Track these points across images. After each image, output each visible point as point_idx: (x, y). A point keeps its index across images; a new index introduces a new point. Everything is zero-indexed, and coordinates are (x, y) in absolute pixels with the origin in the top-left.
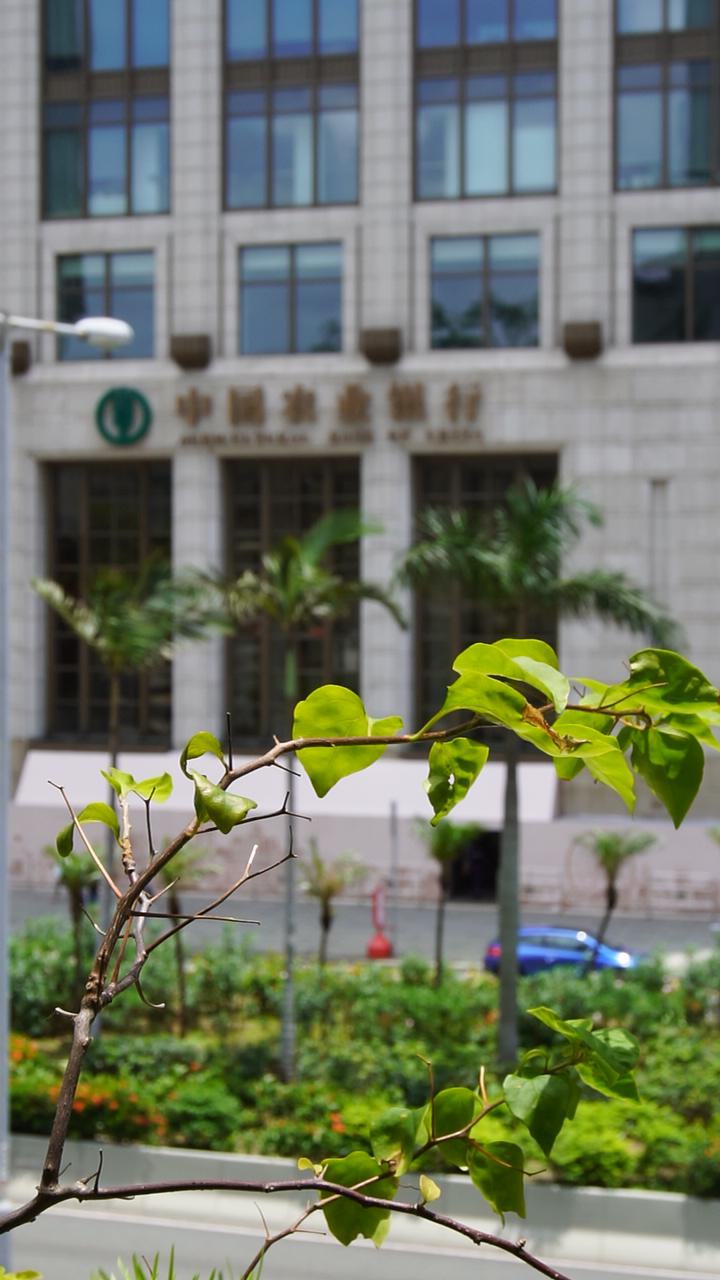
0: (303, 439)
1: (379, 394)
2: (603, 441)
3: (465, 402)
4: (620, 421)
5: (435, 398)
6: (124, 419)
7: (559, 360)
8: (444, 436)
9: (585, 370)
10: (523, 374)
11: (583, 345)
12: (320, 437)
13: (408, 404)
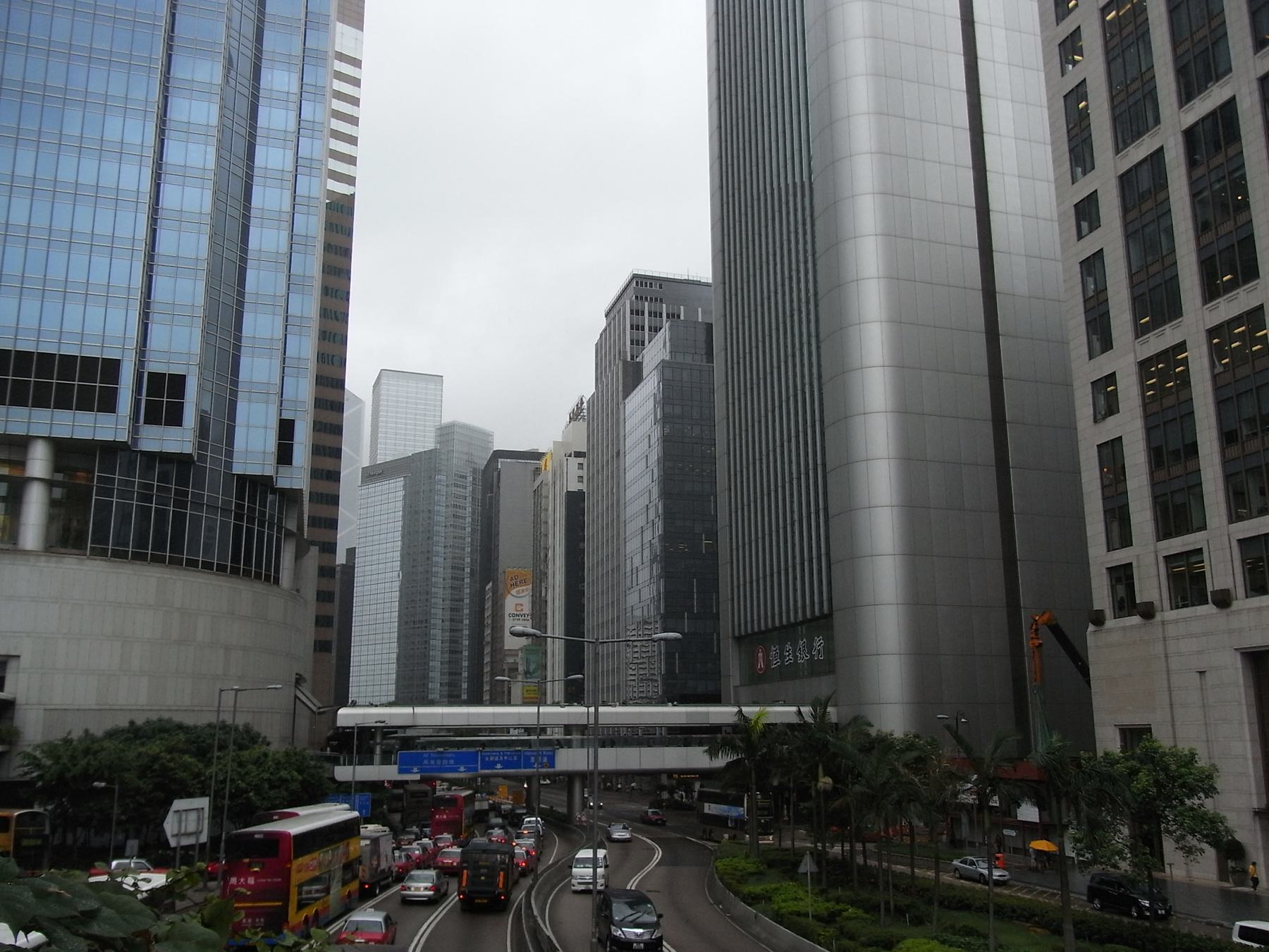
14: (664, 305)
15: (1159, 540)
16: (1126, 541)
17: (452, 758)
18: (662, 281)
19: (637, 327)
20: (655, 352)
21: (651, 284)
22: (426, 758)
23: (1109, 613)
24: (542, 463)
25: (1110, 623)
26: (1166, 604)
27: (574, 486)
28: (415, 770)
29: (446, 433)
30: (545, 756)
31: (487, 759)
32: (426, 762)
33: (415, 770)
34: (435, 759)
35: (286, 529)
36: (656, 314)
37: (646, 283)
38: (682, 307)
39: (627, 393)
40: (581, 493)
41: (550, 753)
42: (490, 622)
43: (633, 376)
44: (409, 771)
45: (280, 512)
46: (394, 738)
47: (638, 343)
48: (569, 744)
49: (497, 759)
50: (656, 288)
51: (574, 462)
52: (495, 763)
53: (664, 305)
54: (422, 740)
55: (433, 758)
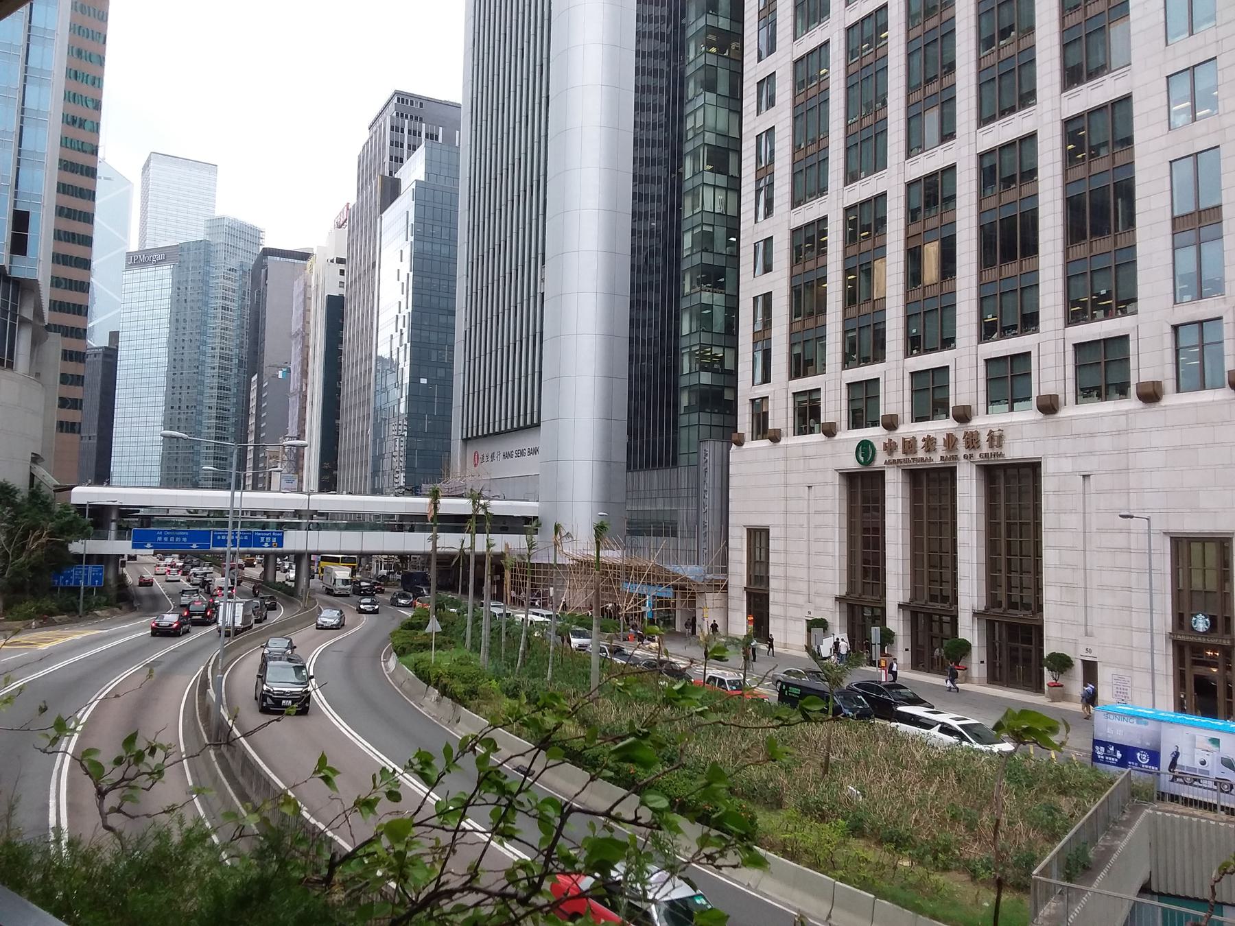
0: (931, 460)
1: (960, 436)
2: (1059, 456)
3: (996, 439)
4: (1066, 445)
5: (984, 438)
6: (865, 455)
7: (1040, 415)
8: (986, 455)
9: (1051, 419)
10: (1022, 423)
11: (1049, 406)
12: (936, 459)
13: (972, 441)
14: (424, 125)
15: (791, 378)
16: (766, 379)
18: (423, 101)
19: (396, 144)
20: (414, 170)
21: (412, 102)
22: (160, 536)
23: (748, 436)
24: (308, 263)
25: (749, 444)
26: (791, 431)
27: (336, 292)
28: (149, 545)
29: (215, 224)
30: (274, 536)
31: (219, 537)
32: (160, 539)
33: (149, 545)
34: (169, 536)
35: (20, 316)
36: (415, 133)
37: (407, 100)
38: (441, 128)
39: (383, 208)
40: (341, 298)
42: (254, 412)
43: (391, 190)
44: (143, 547)
45: (15, 300)
46: (137, 516)
47: (398, 160)
48: (297, 527)
50: (416, 106)
53: (424, 125)
54: (156, 518)
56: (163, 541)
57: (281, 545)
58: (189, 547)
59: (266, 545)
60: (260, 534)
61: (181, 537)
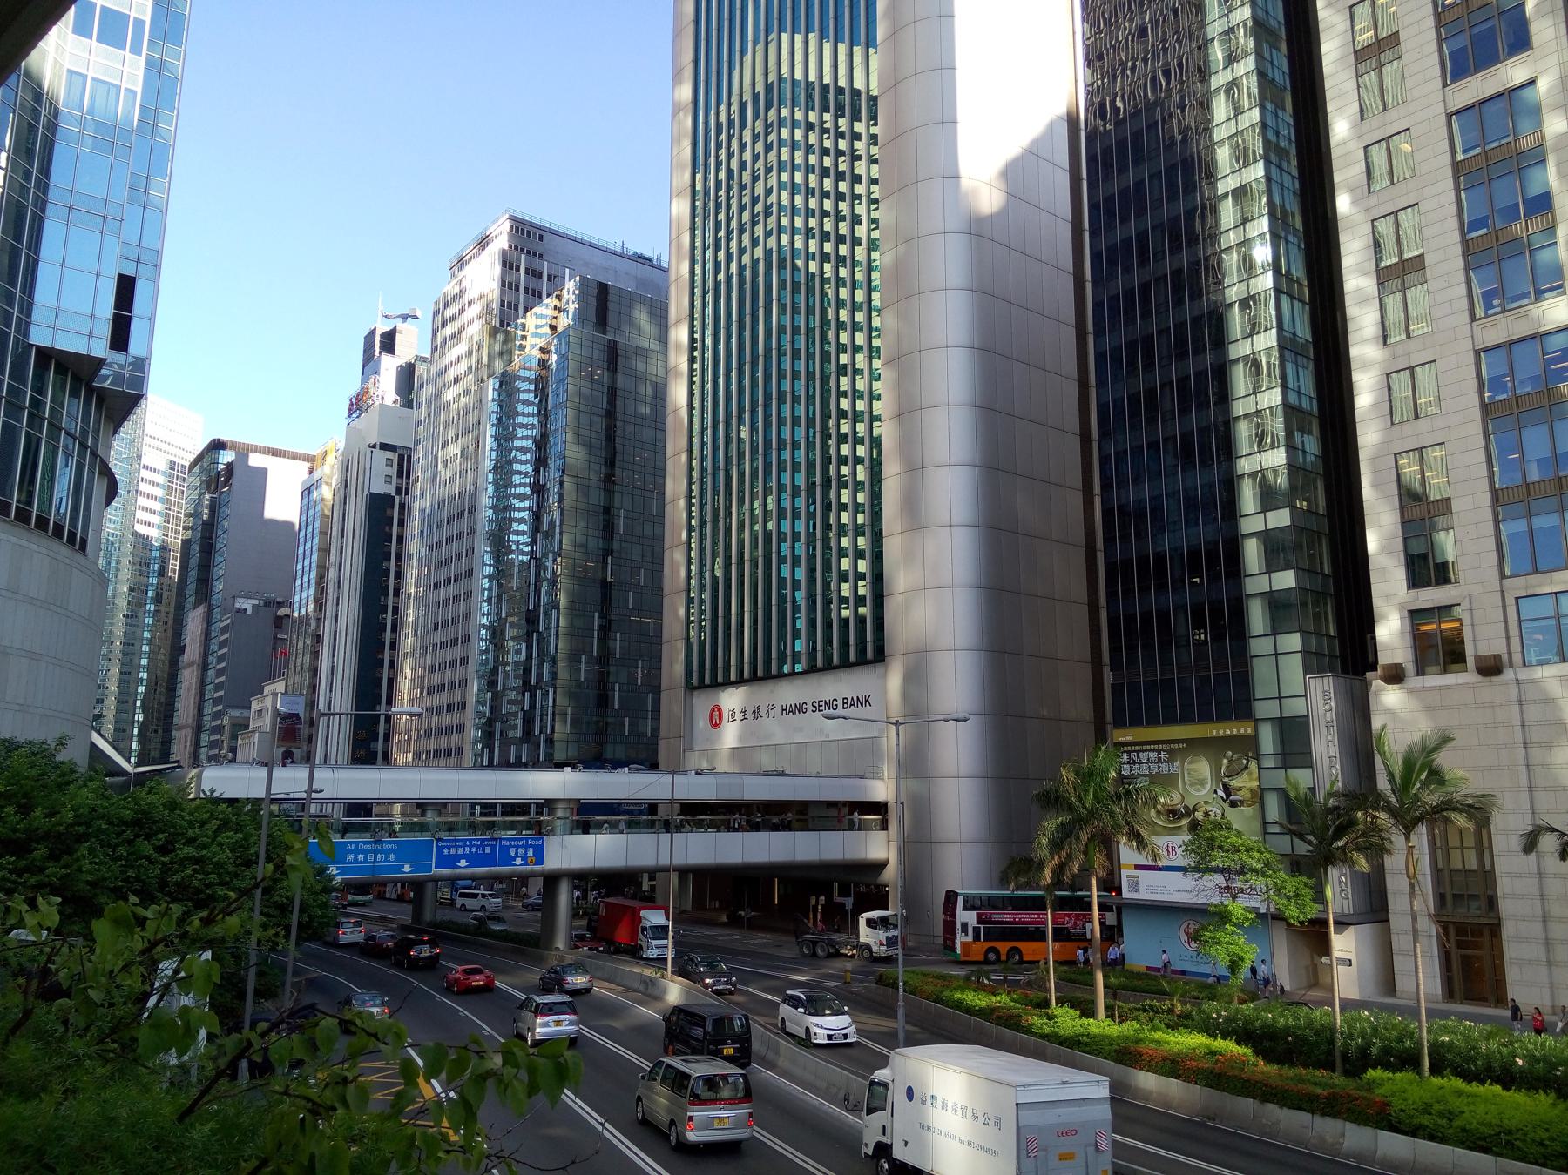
17: (391, 851)
22: (350, 852)
27: (380, 488)
30: (531, 846)
31: (446, 851)
32: (350, 857)
34: (365, 853)
37: (523, 230)
41: (537, 843)
49: (460, 851)
51: (381, 456)
52: (457, 858)
55: (362, 852)
56: (356, 860)
57: (540, 861)
58: (398, 869)
59: (518, 861)
60: (508, 843)
61: (386, 852)
